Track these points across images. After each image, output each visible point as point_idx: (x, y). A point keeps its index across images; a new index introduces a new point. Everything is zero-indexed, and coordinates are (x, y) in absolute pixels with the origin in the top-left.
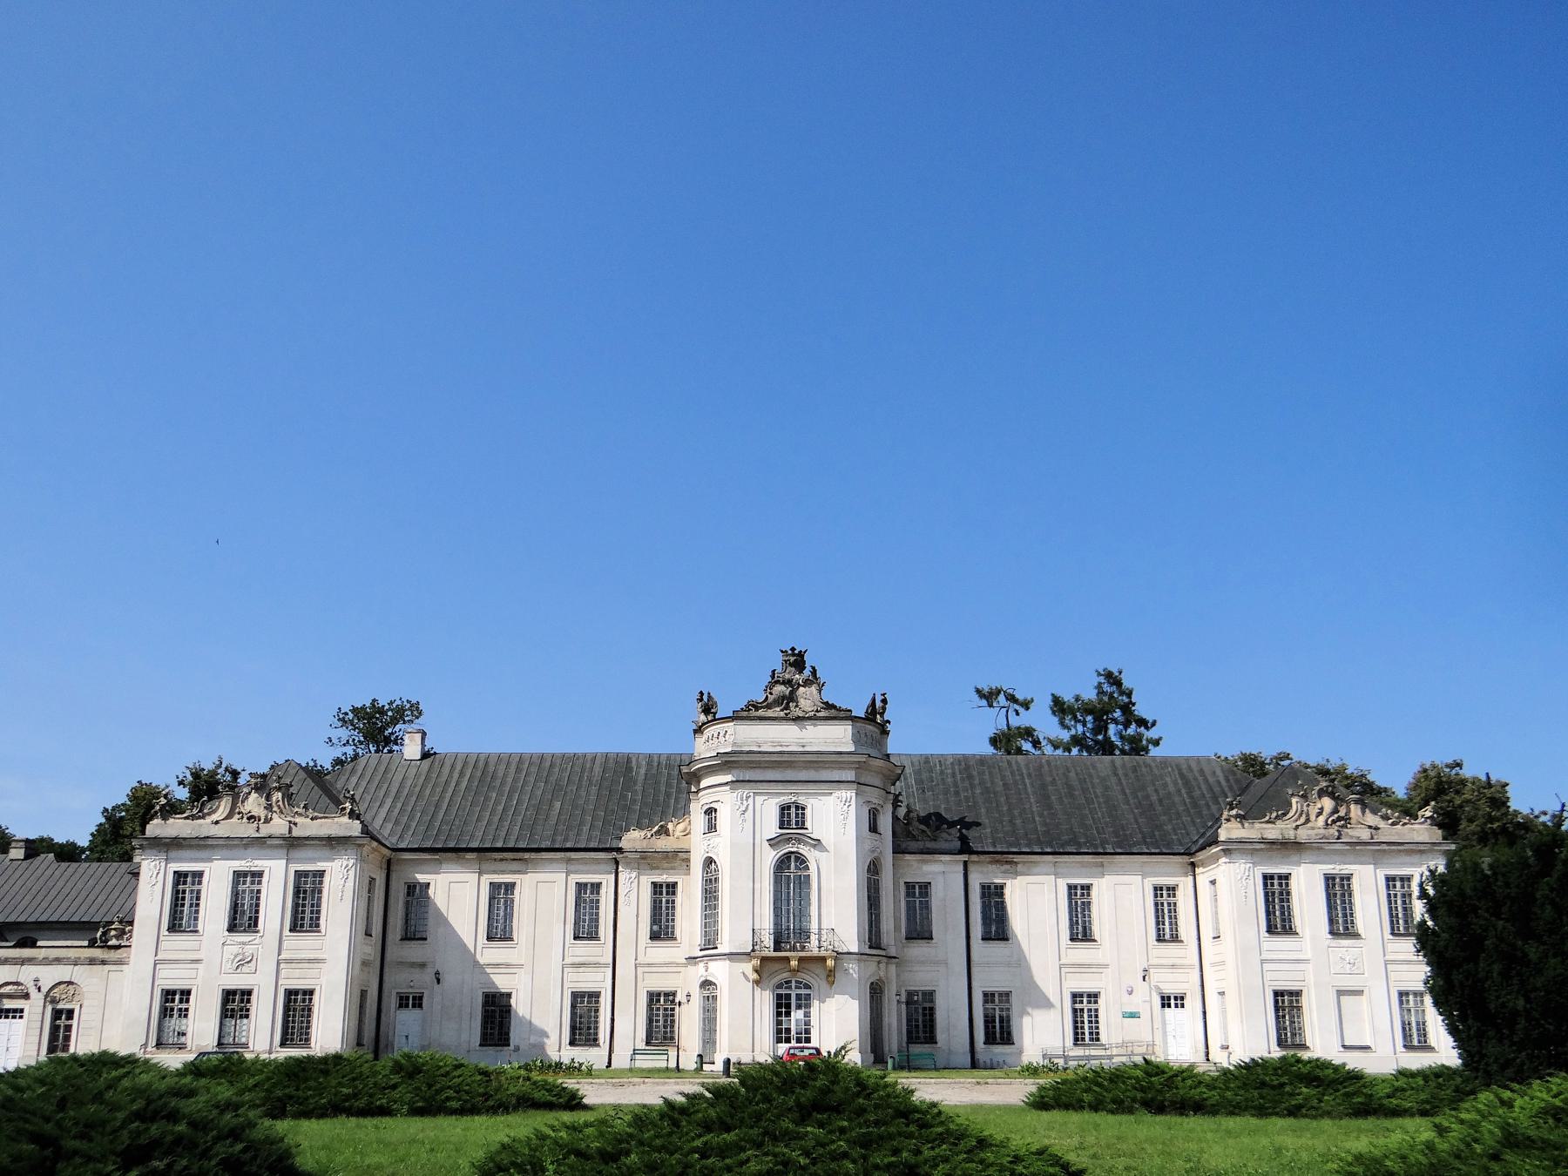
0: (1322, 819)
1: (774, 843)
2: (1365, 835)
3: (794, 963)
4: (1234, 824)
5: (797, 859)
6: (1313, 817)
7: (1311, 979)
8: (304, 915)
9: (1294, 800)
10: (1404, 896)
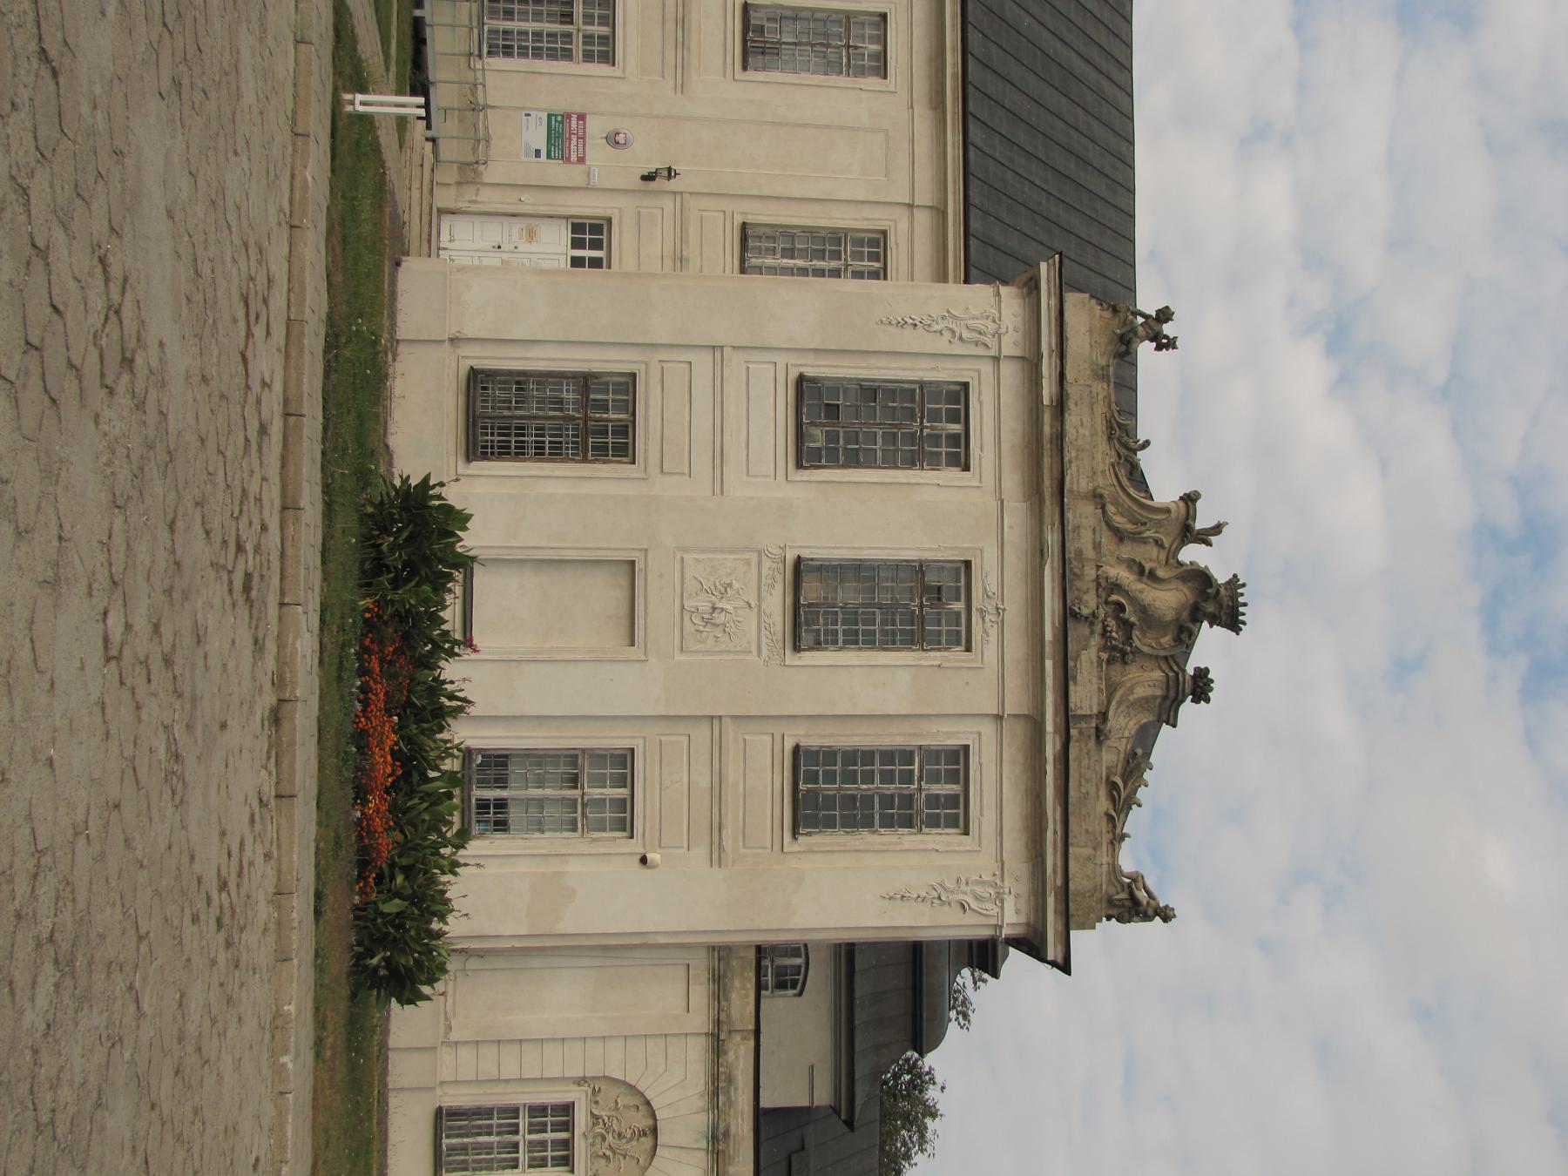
2: (1085, 697)
6: (1126, 551)
10: (908, 800)
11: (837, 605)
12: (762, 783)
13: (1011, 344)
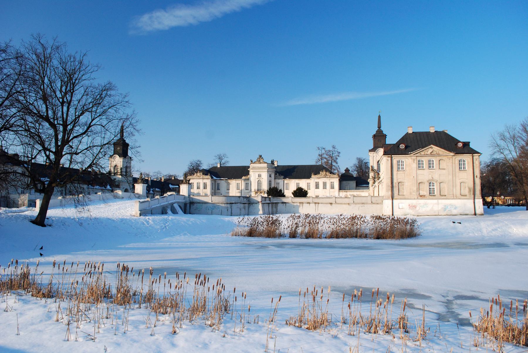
8: (205, 187)
12: (332, 190)
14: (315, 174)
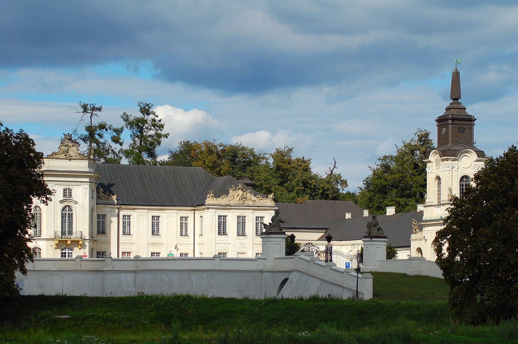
0: (238, 198)
1: (61, 202)
2: (251, 203)
3: (69, 242)
4: (211, 199)
5: (69, 208)
6: (235, 197)
7: (230, 249)
9: (230, 191)
11: (241, 232)
13: (214, 210)
14: (217, 195)
